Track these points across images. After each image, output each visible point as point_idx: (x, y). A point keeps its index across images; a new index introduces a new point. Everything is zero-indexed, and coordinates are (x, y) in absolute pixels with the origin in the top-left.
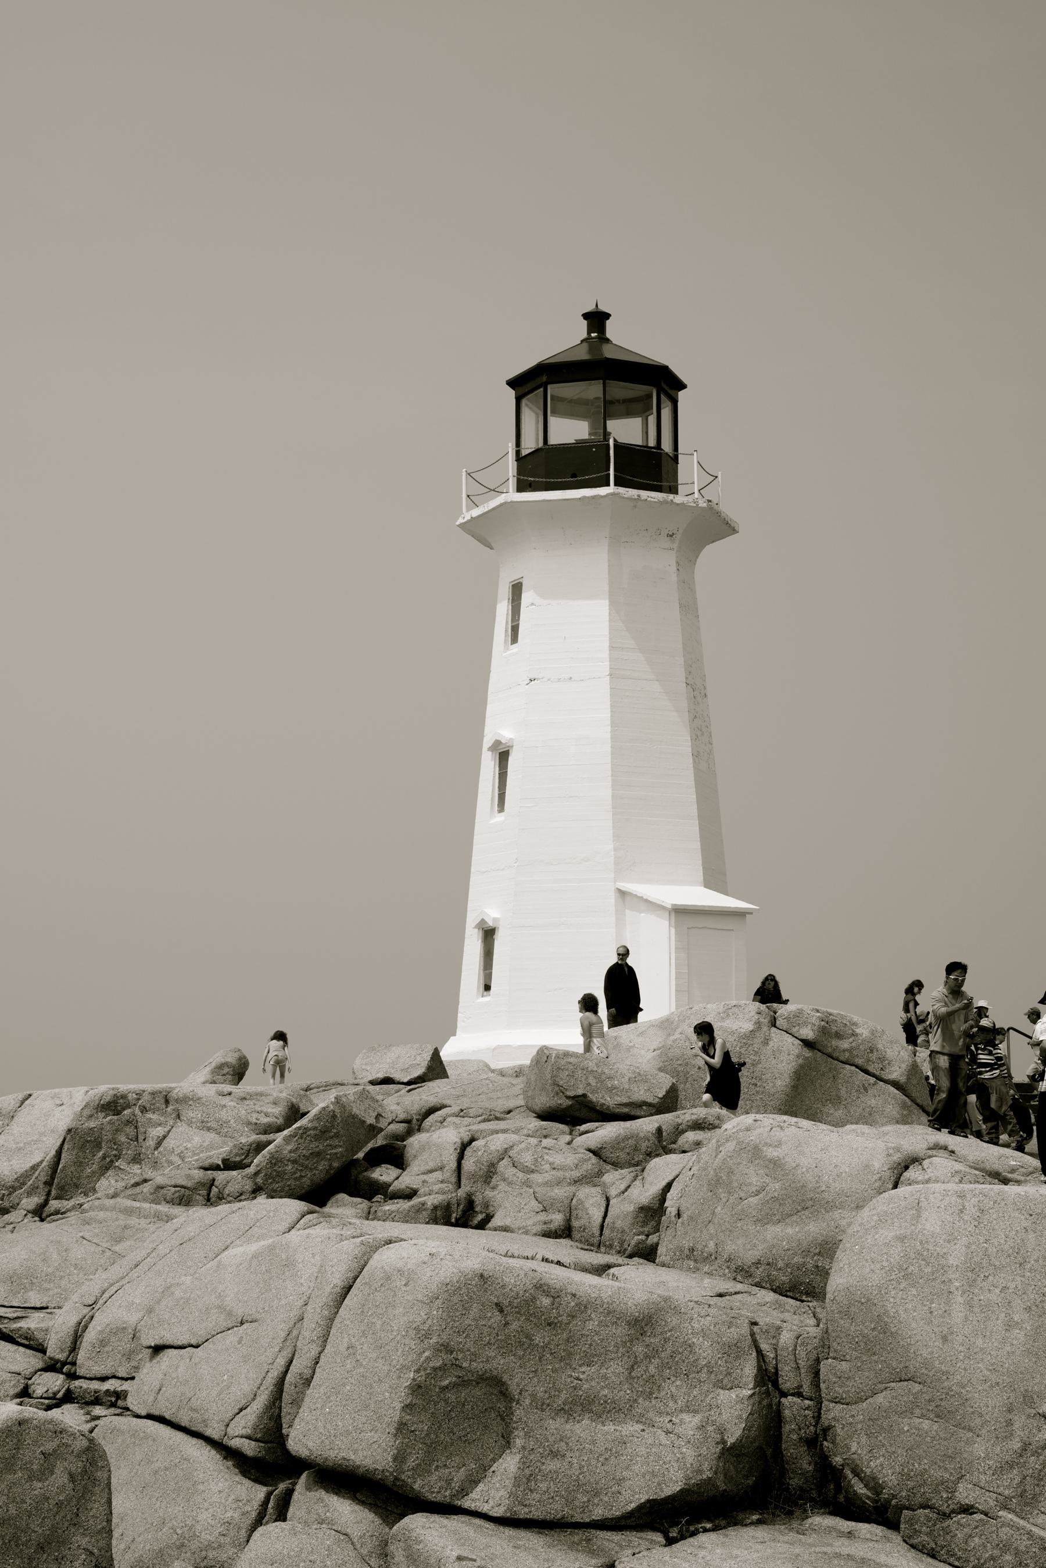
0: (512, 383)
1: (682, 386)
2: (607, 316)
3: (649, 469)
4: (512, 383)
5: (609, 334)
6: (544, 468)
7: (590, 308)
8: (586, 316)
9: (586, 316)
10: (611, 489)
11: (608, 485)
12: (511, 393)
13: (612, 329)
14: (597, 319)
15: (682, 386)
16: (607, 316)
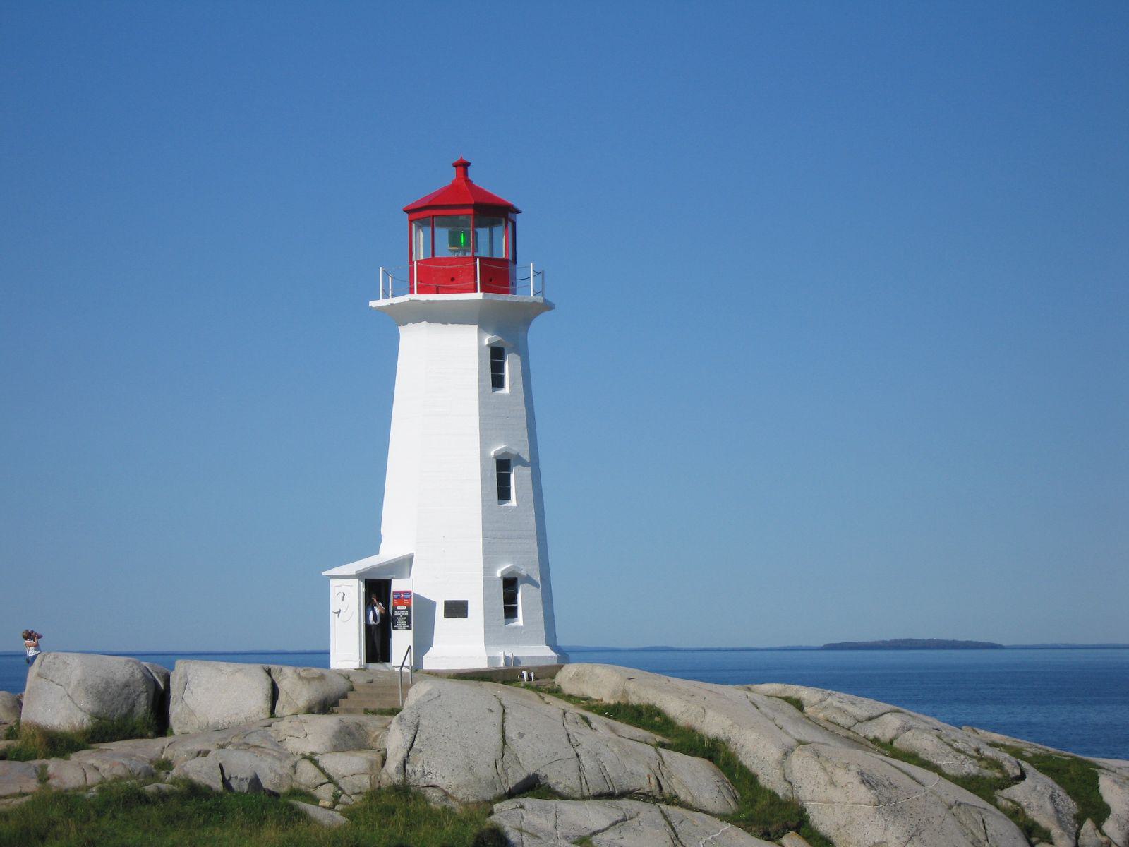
0: (408, 211)
1: (518, 212)
2: (469, 164)
3: (497, 275)
4: (408, 211)
5: (471, 176)
6: (433, 276)
7: (456, 159)
8: (455, 165)
9: (455, 165)
10: (478, 296)
11: (476, 291)
12: (406, 216)
13: (474, 175)
14: (463, 166)
15: (518, 212)
16: (469, 164)
